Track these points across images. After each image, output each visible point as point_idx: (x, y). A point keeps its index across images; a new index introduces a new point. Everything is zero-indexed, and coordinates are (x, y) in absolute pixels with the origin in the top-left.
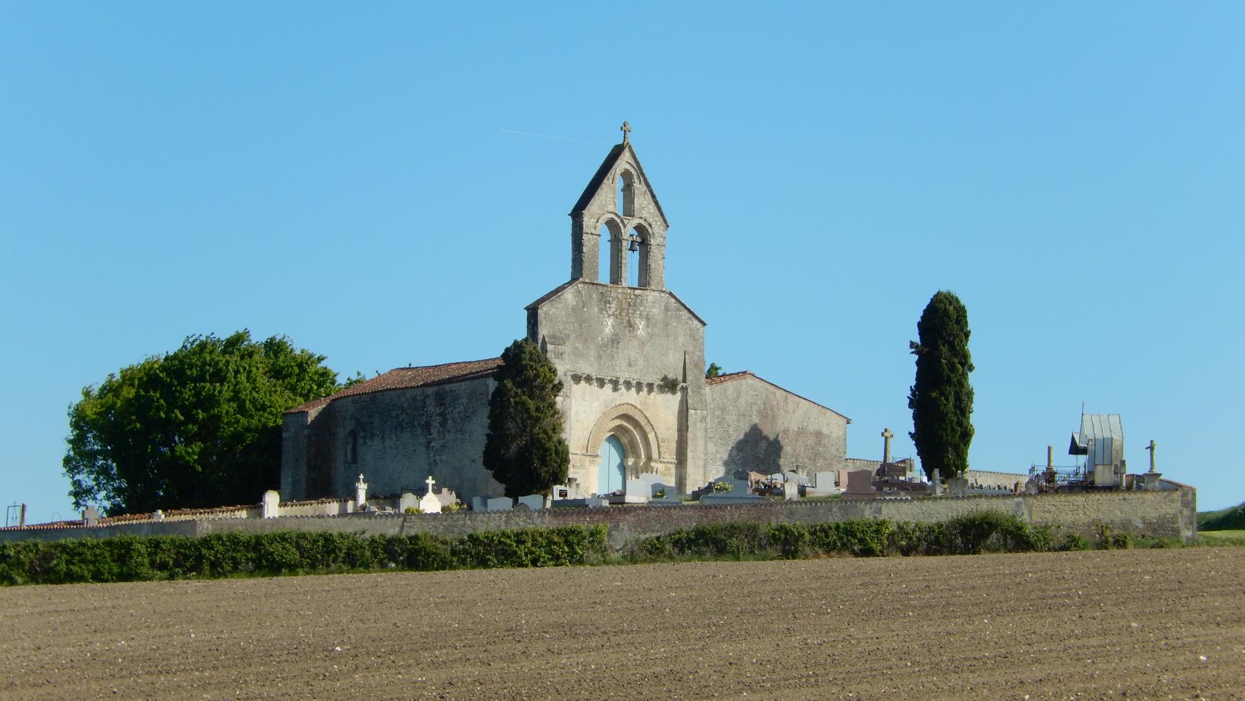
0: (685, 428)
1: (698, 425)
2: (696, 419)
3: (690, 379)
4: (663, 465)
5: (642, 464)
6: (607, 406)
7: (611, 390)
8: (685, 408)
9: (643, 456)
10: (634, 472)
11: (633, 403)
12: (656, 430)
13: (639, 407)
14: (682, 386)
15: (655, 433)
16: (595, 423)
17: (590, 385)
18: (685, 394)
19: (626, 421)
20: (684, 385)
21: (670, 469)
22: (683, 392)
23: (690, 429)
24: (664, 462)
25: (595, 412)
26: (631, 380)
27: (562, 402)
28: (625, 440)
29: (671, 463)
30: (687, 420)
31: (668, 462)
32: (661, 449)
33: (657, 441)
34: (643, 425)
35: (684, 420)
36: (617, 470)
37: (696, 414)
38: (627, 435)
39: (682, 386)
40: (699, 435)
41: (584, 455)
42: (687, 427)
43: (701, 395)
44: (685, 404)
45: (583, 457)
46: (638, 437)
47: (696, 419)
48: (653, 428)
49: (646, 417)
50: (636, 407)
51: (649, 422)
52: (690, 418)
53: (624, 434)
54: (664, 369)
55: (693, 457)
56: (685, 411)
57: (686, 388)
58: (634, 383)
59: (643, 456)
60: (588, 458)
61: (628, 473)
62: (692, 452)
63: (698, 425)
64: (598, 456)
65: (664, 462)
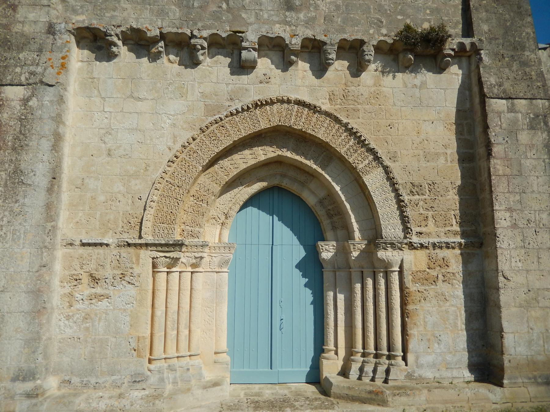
0: (482, 151)
1: (524, 137)
2: (514, 122)
3: (485, 28)
4: (422, 254)
5: (355, 254)
6: (209, 110)
7: (228, 70)
8: (477, 100)
9: (357, 235)
10: (341, 275)
11: (307, 99)
12: (387, 162)
13: (326, 107)
14: (462, 45)
15: (387, 170)
16: (170, 155)
17: (155, 58)
18: (473, 67)
19: (295, 150)
20: (467, 41)
21: (445, 263)
22: (470, 64)
23: (496, 150)
24: (422, 246)
25: (174, 125)
26: (286, 36)
27: (25, 101)
28: (311, 200)
29: (448, 246)
30: (486, 127)
31: (434, 245)
32: (409, 212)
33: (396, 191)
34: (342, 151)
35: (479, 130)
36: (298, 273)
37: (512, 110)
38: (313, 185)
39: (462, 45)
40: (528, 163)
41: (129, 245)
42: (488, 146)
43: (524, 64)
44: (476, 89)
45: (125, 252)
46: (338, 188)
47: (514, 122)
48: (377, 158)
49: (352, 133)
50: (314, 109)
51: (361, 142)
52: (493, 121)
53: (303, 184)
54: (402, 13)
55: (514, 226)
56: (478, 107)
57: (476, 50)
58: (296, 43)
59: (357, 235)
60: (146, 255)
61: (328, 276)
62: (509, 209)
63: (524, 137)
64: (179, 245)
65: (422, 246)
